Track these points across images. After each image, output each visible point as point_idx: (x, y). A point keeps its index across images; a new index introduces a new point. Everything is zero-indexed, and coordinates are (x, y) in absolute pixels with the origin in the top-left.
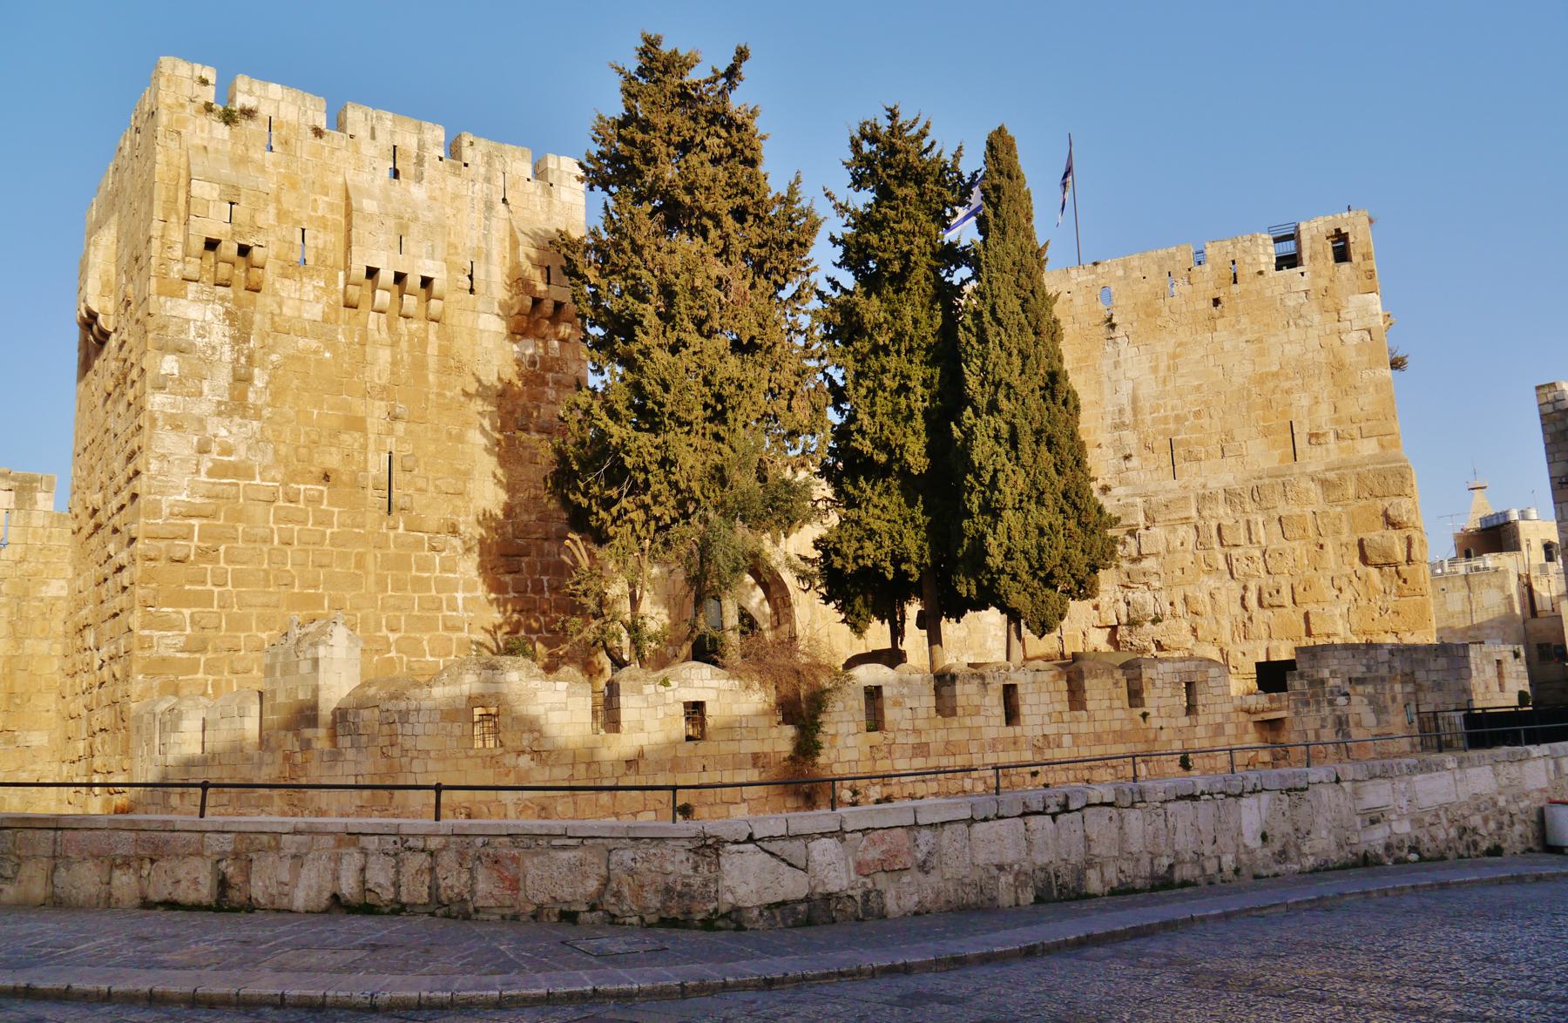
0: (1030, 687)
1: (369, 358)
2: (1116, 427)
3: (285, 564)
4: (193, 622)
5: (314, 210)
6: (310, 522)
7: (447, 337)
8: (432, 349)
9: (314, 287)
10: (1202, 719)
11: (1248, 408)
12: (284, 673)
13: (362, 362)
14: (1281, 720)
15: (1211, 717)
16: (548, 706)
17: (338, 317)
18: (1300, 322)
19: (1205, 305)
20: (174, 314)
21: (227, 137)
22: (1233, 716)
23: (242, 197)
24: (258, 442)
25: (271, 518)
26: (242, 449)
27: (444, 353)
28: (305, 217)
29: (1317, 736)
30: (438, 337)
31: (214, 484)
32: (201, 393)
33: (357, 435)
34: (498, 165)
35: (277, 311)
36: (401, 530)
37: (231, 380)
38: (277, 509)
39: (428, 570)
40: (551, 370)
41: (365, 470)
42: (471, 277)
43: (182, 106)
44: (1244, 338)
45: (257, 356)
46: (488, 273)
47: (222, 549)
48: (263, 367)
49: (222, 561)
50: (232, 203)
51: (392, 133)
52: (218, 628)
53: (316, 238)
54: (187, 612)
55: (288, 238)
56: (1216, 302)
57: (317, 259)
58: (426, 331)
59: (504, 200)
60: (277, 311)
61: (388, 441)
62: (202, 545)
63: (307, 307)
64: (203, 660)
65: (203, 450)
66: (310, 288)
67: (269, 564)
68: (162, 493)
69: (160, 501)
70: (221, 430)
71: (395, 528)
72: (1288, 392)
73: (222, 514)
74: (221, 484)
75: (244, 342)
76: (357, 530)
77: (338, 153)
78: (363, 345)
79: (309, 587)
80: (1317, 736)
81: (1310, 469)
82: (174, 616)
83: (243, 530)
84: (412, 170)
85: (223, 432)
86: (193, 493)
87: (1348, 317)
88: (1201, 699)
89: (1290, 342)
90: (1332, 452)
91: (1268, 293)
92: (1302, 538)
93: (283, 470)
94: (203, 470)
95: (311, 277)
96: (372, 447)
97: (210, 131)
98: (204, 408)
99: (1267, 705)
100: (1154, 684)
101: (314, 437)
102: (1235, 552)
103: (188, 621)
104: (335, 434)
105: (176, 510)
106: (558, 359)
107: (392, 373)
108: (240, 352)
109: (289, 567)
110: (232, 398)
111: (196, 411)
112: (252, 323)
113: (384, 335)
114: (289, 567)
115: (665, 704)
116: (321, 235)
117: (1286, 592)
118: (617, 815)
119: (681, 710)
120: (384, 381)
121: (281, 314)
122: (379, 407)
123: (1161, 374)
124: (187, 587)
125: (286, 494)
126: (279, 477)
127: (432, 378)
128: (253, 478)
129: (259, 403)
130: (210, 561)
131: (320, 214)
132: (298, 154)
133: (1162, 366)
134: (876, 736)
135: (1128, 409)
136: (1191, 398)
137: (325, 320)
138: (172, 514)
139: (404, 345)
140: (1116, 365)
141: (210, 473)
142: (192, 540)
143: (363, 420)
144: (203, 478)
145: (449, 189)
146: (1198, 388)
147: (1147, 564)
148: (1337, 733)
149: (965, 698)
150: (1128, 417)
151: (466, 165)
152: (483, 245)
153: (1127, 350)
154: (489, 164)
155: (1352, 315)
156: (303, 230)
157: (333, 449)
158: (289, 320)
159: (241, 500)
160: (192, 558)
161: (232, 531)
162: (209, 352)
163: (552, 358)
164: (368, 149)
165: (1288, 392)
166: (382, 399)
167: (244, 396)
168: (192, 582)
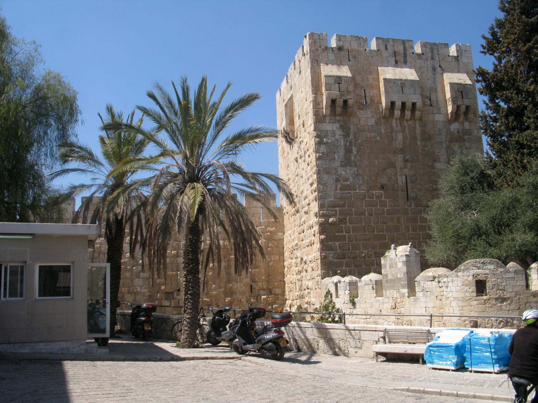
1: (394, 138)
4: (340, 247)
5: (368, 81)
6: (379, 206)
7: (424, 124)
8: (418, 132)
9: (371, 112)
12: (390, 267)
20: (322, 129)
24: (357, 176)
25: (364, 205)
26: (351, 179)
27: (423, 133)
31: (343, 193)
32: (335, 158)
33: (392, 169)
34: (436, 52)
36: (413, 207)
38: (365, 202)
39: (425, 222)
40: (466, 134)
41: (397, 183)
42: (430, 100)
43: (317, 50)
46: (437, 97)
47: (348, 218)
49: (348, 223)
50: (339, 84)
51: (393, 46)
52: (349, 250)
53: (369, 92)
54: (337, 244)
57: (371, 101)
58: (415, 124)
59: (440, 66)
61: (405, 170)
62: (340, 217)
64: (344, 262)
65: (337, 181)
66: (370, 112)
67: (365, 223)
71: (411, 206)
74: (345, 193)
76: (396, 208)
77: (374, 58)
78: (391, 133)
79: (381, 232)
82: (333, 245)
83: (354, 211)
85: (344, 173)
86: (335, 198)
94: (338, 188)
95: (370, 108)
96: (399, 174)
97: (328, 57)
98: (337, 164)
101: (377, 171)
103: (338, 247)
104: (384, 170)
105: (330, 205)
106: (469, 129)
107: (404, 143)
108: (347, 141)
109: (372, 224)
110: (346, 159)
111: (334, 166)
112: (350, 129)
113: (399, 127)
114: (372, 224)
116: (371, 91)
120: (400, 147)
121: (360, 124)
124: (337, 234)
125: (368, 195)
126: (365, 189)
127: (419, 143)
128: (356, 190)
129: (355, 160)
131: (370, 82)
132: (360, 61)
137: (376, 124)
138: (329, 207)
139: (407, 131)
141: (341, 190)
152: (434, 86)
154: (432, 52)
156: (365, 90)
157: (384, 176)
159: (353, 199)
160: (338, 223)
162: (336, 142)
163: (466, 130)
164: (385, 54)
166: (401, 154)
167: (350, 159)
168: (338, 232)
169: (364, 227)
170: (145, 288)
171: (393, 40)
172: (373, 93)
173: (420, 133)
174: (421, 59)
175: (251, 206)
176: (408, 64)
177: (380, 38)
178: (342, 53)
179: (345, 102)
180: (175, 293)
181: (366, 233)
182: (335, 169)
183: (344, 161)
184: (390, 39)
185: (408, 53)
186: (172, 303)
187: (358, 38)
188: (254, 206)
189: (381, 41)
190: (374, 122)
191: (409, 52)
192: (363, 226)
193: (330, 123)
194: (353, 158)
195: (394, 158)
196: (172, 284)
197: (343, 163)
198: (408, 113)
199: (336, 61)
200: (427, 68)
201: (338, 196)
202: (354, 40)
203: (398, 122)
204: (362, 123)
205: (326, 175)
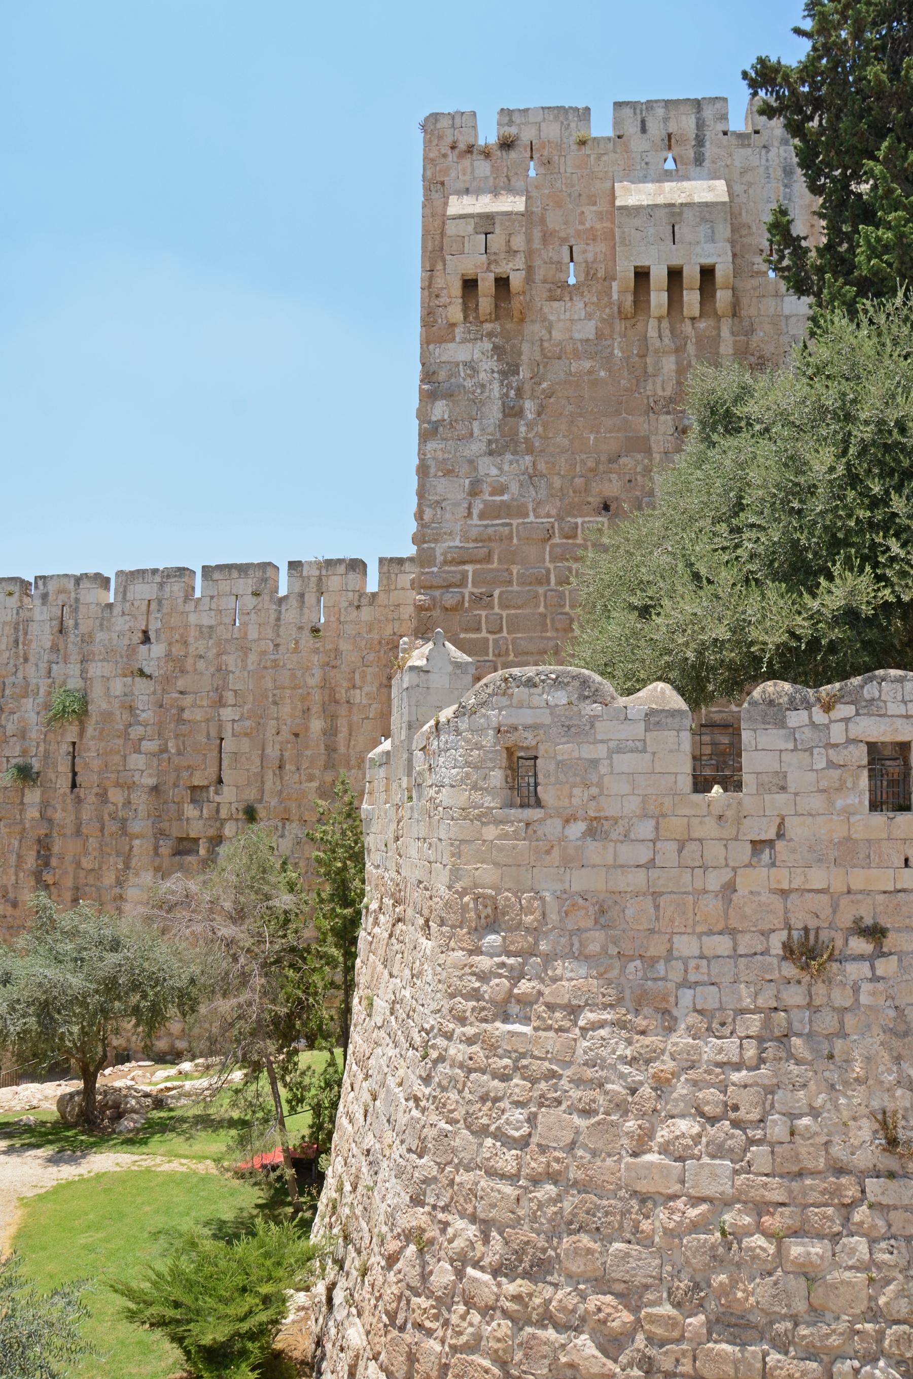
1: (650, 370)
3: (564, 606)
5: (582, 223)
13: (643, 376)
16: (613, 744)
17: (612, 331)
20: (443, 359)
21: (488, 173)
23: (497, 225)
25: (547, 557)
26: (514, 488)
28: (571, 232)
30: (733, 333)
31: (486, 526)
32: (472, 435)
33: (639, 456)
35: (547, 337)
37: (500, 416)
38: (553, 546)
43: (445, 156)
45: (527, 387)
47: (496, 593)
48: (533, 397)
51: (666, 120)
53: (585, 252)
55: (555, 259)
58: (718, 328)
60: (547, 337)
62: (476, 591)
63: (578, 326)
66: (581, 305)
67: (546, 607)
68: (436, 541)
69: (434, 549)
70: (489, 468)
73: (496, 557)
74: (493, 525)
75: (513, 375)
77: (605, 158)
78: (643, 356)
84: (691, 154)
85: (494, 471)
86: (465, 538)
93: (558, 504)
94: (475, 512)
101: (591, 464)
104: (614, 459)
105: (449, 557)
108: (509, 386)
110: (503, 436)
111: (467, 453)
112: (520, 354)
113: (666, 341)
115: (830, 746)
116: (590, 248)
118: (732, 932)
119: (860, 754)
120: (668, 393)
122: (665, 422)
124: (462, 636)
125: (561, 529)
126: (554, 512)
128: (527, 515)
129: (530, 436)
130: (484, 608)
131: (588, 226)
132: (562, 170)
137: (599, 336)
138: (446, 562)
141: (482, 516)
142: (466, 586)
143: (647, 439)
144: (475, 521)
145: (737, 164)
151: (757, 132)
156: (571, 248)
157: (614, 476)
158: (560, 343)
159: (515, 541)
160: (467, 605)
161: (506, 574)
164: (638, 144)
166: (668, 413)
168: (467, 630)
169: (544, 616)
170: (150, 776)
171: (668, 103)
172: (596, 254)
173: (731, 352)
174: (749, 145)
175: (393, 587)
176: (707, 164)
177: (627, 103)
178: (513, 155)
179: (502, 283)
180: (212, 789)
181: (549, 634)
182: (471, 462)
183: (497, 441)
184: (657, 101)
185: (708, 134)
186: (205, 811)
187: (561, 112)
188: (399, 587)
189: (627, 112)
190: (594, 331)
191: (713, 131)
192: (540, 614)
193: (464, 341)
194: (523, 429)
195: (646, 426)
196: (205, 769)
197: (494, 446)
198: (691, 298)
199: (495, 178)
200: (767, 168)
201: (474, 533)
202: (552, 117)
203: (665, 324)
204: (557, 335)
205: (443, 479)
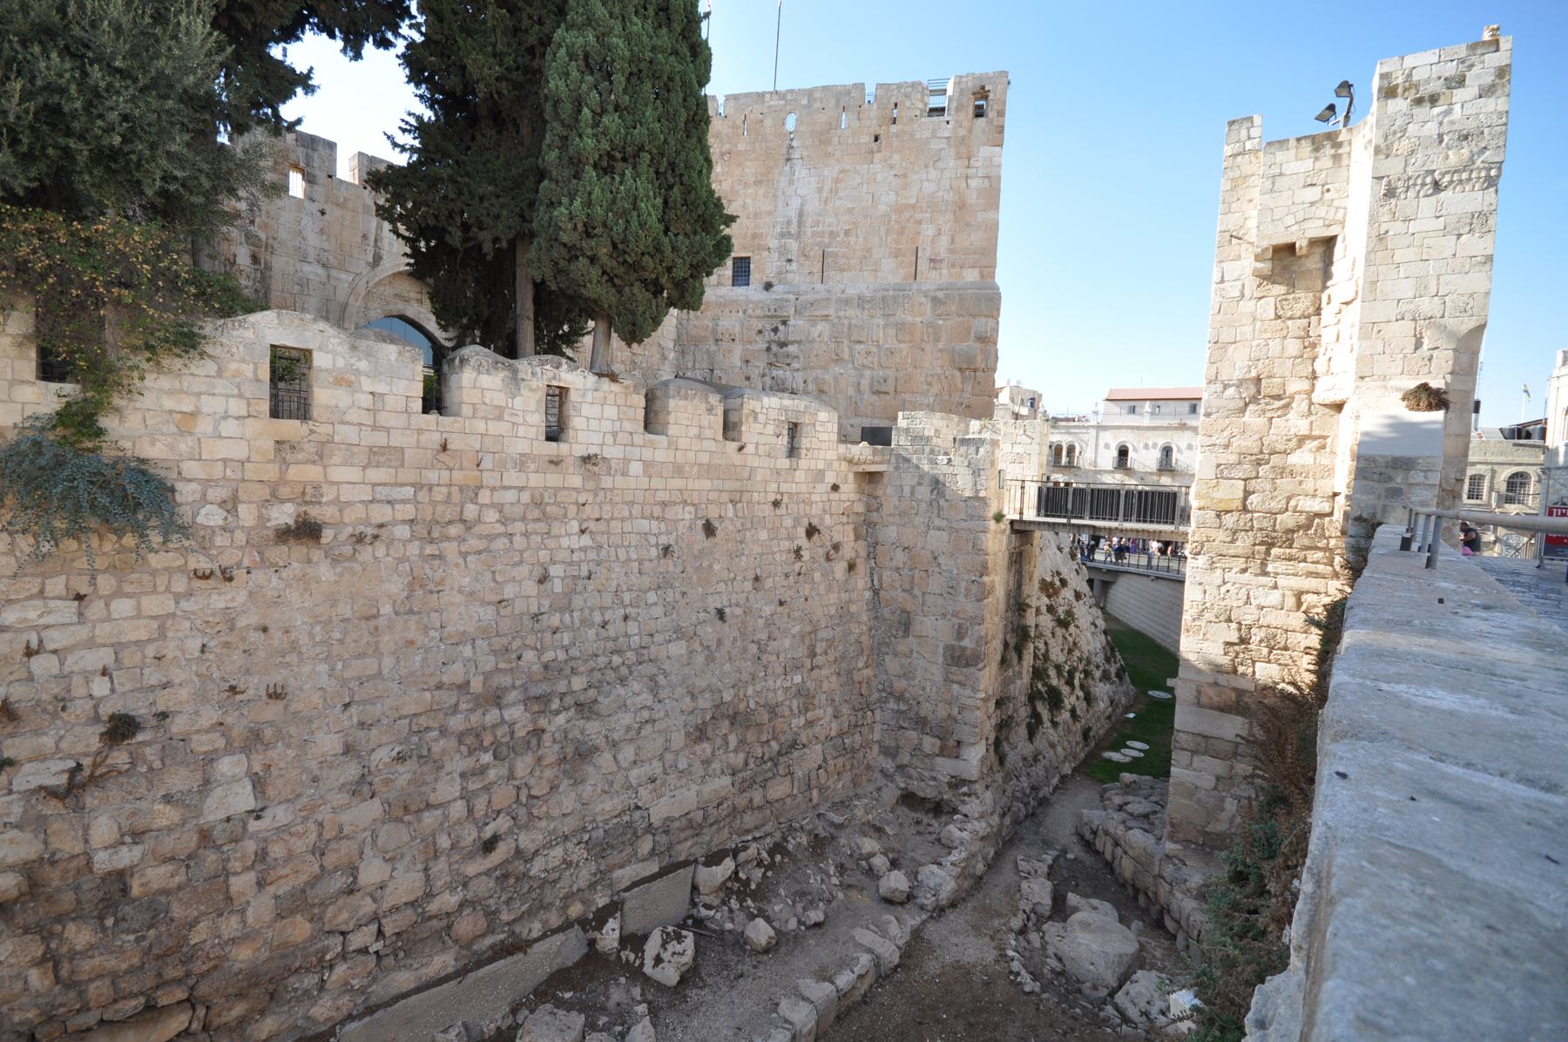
0: (589, 394)
2: (783, 235)
10: (803, 463)
11: (887, 231)
14: (880, 474)
15: (813, 462)
18: (938, 164)
19: (867, 139)
22: (836, 465)
29: (912, 493)
44: (893, 172)
56: (876, 139)
72: (920, 222)
80: (912, 493)
81: (924, 288)
87: (977, 164)
88: (804, 442)
89: (928, 180)
90: (944, 275)
91: (918, 136)
92: (910, 341)
99: (870, 457)
100: (756, 419)
102: (858, 347)
117: (891, 381)
123: (824, 195)
133: (826, 188)
134: (290, 428)
135: (795, 221)
136: (845, 218)
140: (791, 182)
146: (851, 211)
147: (792, 349)
148: (932, 491)
149: (477, 392)
150: (794, 229)
153: (801, 171)
155: (979, 164)
165: (920, 222)
